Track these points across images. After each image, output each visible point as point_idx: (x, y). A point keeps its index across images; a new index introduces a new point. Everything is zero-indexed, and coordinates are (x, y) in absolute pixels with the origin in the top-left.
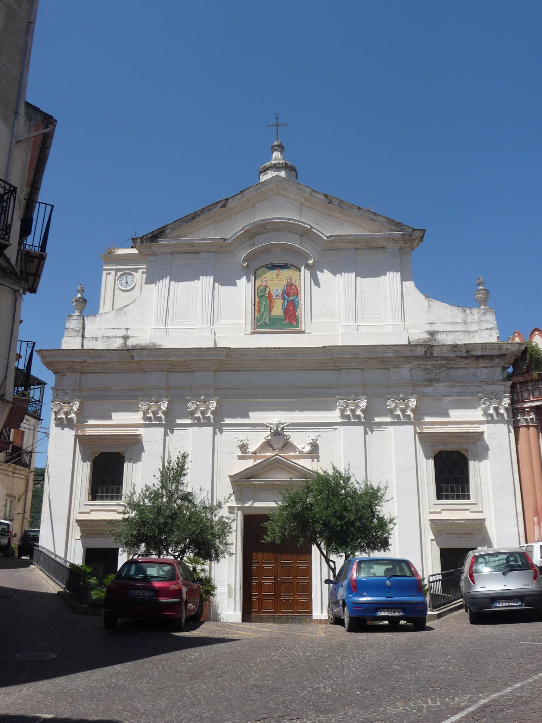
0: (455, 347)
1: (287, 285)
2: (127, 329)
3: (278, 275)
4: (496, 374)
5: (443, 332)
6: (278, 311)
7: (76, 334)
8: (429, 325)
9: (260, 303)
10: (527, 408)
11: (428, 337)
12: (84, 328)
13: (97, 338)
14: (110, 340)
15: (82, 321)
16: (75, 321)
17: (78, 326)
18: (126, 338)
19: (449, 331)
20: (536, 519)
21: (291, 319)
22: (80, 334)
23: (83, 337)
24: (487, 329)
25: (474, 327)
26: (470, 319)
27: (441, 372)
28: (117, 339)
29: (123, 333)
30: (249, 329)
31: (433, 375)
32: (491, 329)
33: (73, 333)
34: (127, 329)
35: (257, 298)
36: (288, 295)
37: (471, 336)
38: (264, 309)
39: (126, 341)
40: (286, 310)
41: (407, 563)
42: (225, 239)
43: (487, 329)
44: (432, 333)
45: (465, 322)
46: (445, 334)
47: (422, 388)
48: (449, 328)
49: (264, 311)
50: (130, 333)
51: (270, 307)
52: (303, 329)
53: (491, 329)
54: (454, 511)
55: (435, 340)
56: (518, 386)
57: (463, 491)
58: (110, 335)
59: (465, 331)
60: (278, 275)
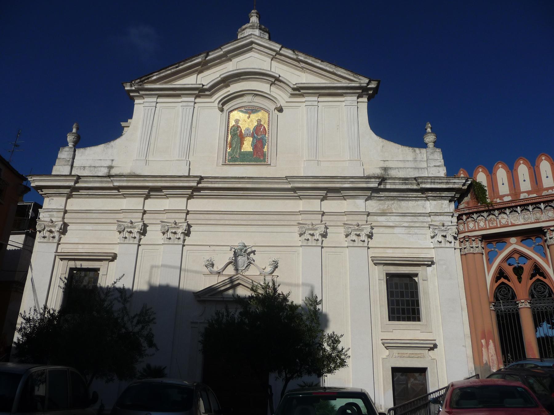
0: (405, 180)
1: (257, 126)
2: (113, 160)
3: (249, 117)
4: (444, 206)
5: (395, 168)
6: (247, 146)
7: (66, 163)
8: (383, 162)
9: (231, 140)
10: (473, 236)
11: (382, 172)
12: (74, 158)
13: (84, 167)
14: (96, 169)
15: (72, 153)
16: (66, 153)
17: (69, 157)
18: (110, 168)
19: (401, 168)
20: (483, 341)
21: (258, 155)
22: (70, 163)
23: (72, 166)
24: (435, 166)
25: (424, 165)
26: (419, 157)
27: (393, 204)
28: (102, 169)
29: (108, 163)
30: (221, 161)
31: (386, 206)
32: (439, 166)
33: (63, 163)
34: (113, 160)
35: (230, 137)
36: (257, 134)
37: (420, 172)
38: (236, 146)
39: (110, 171)
40: (255, 146)
41: (363, 396)
42: (203, 85)
43: (435, 166)
44: (385, 169)
45: (415, 160)
46: (397, 170)
47: (375, 217)
48: (401, 165)
49: (235, 148)
50: (114, 164)
51: (242, 143)
52: (269, 163)
53: (439, 166)
54: (405, 331)
55: (388, 175)
56: (464, 217)
57: (414, 313)
58: (97, 165)
59: (415, 168)
60: (249, 117)
